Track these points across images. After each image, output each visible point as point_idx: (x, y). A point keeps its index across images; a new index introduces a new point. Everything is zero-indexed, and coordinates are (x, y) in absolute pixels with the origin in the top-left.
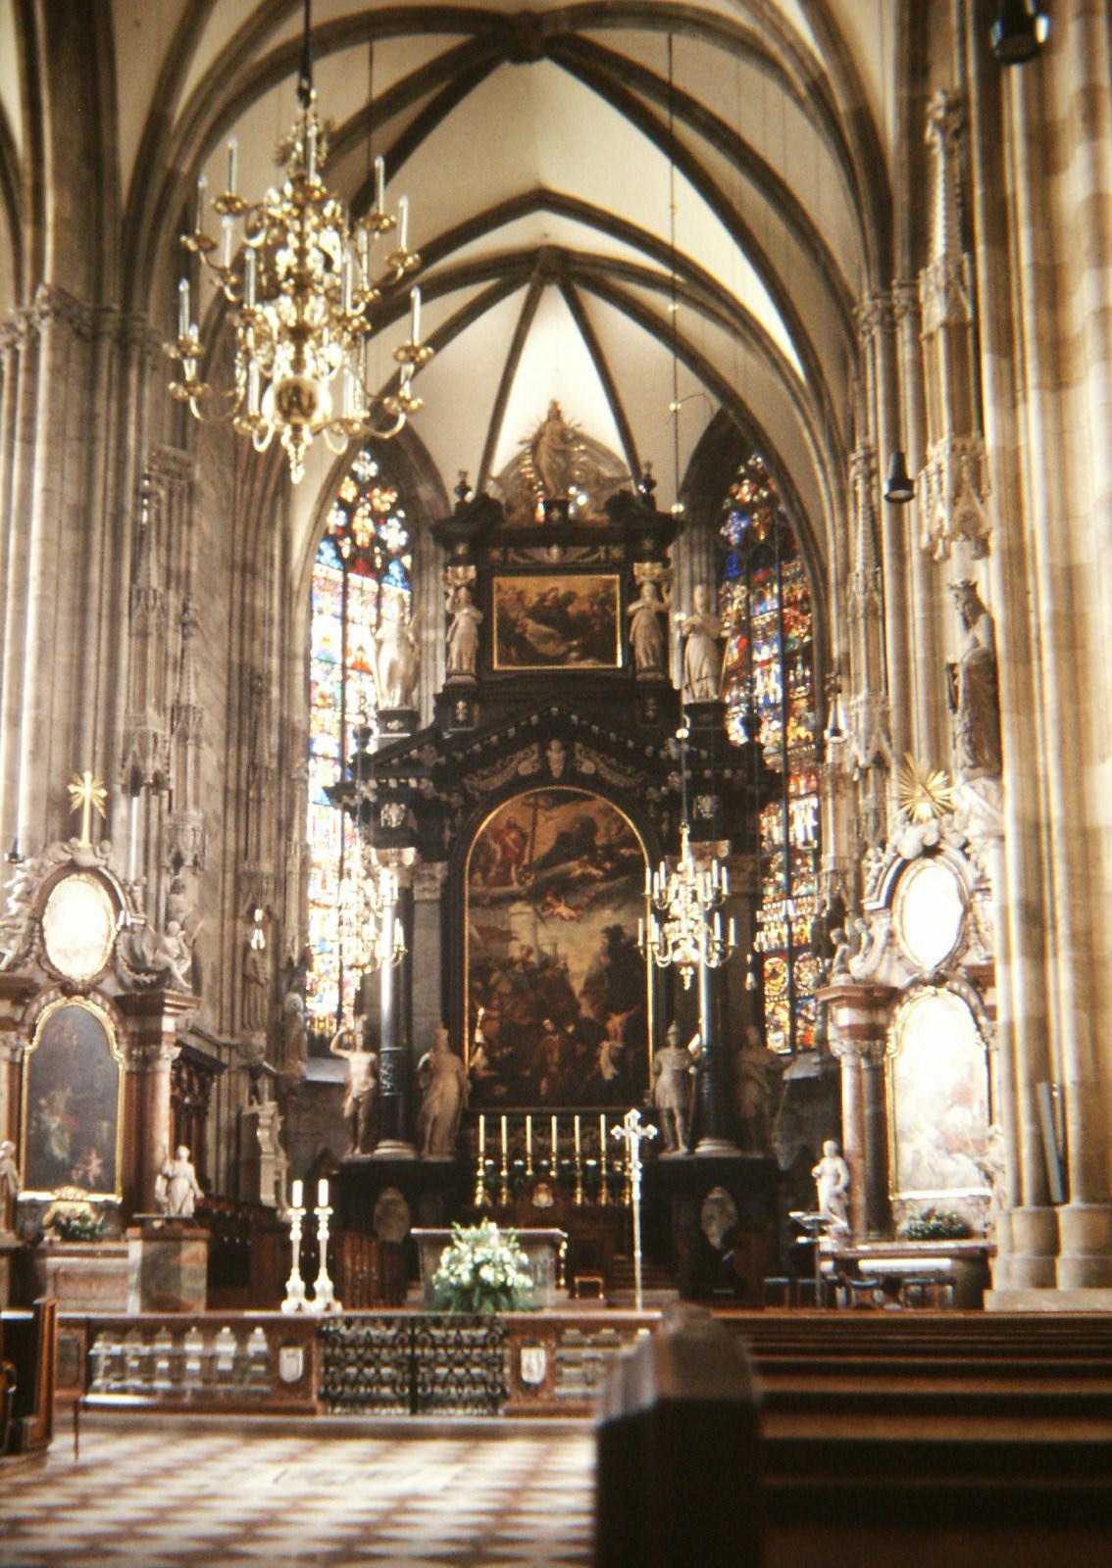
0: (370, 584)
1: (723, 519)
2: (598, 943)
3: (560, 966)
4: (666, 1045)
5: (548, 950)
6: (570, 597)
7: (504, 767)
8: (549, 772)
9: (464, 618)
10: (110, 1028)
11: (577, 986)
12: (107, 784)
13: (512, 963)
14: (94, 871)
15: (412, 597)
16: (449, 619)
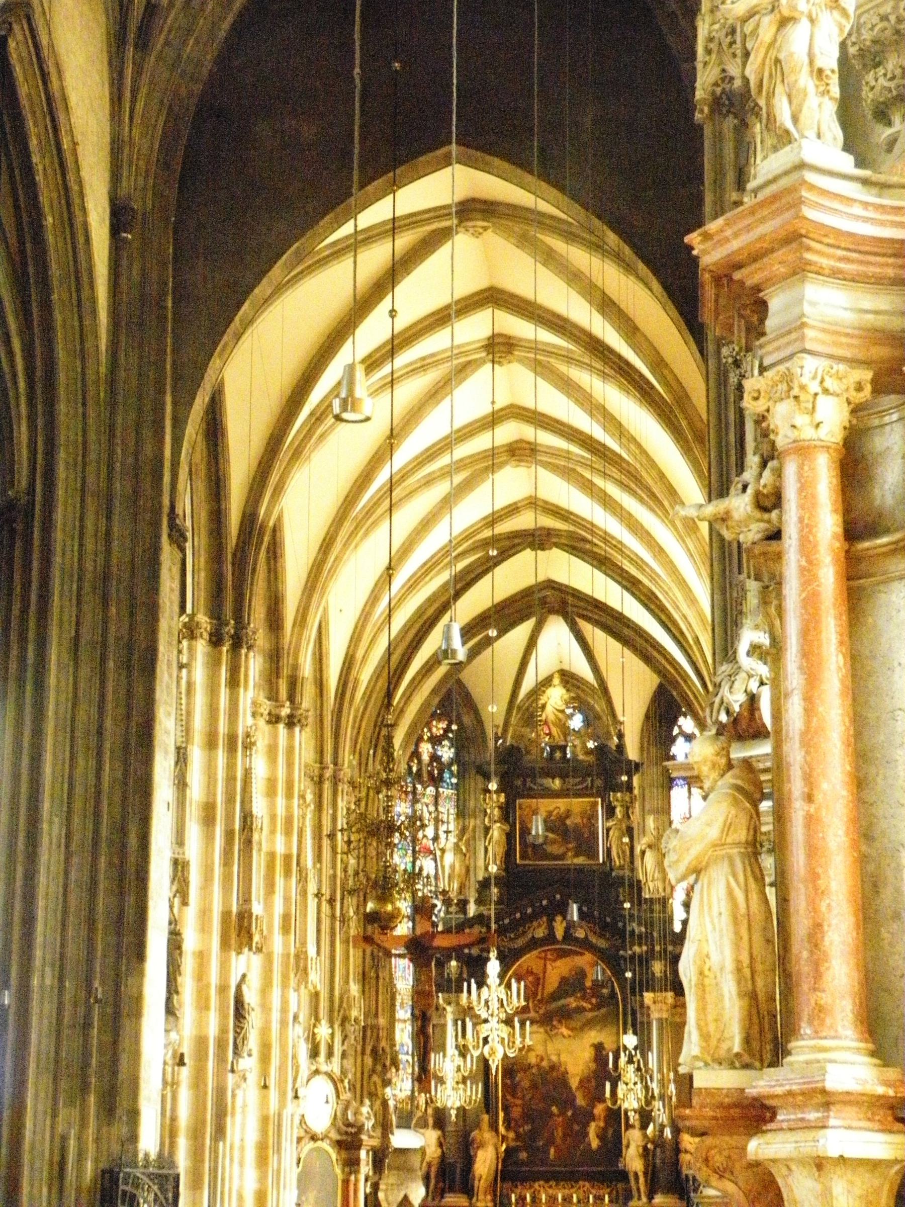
0: (431, 790)
1: (673, 740)
2: (587, 1054)
3: (562, 1069)
4: (633, 1127)
5: (554, 1058)
6: (568, 814)
7: (524, 933)
8: (555, 937)
9: (497, 832)
10: (334, 1156)
11: (574, 1083)
12: (332, 1027)
13: (530, 1066)
14: (326, 1073)
15: (458, 795)
16: (487, 830)
